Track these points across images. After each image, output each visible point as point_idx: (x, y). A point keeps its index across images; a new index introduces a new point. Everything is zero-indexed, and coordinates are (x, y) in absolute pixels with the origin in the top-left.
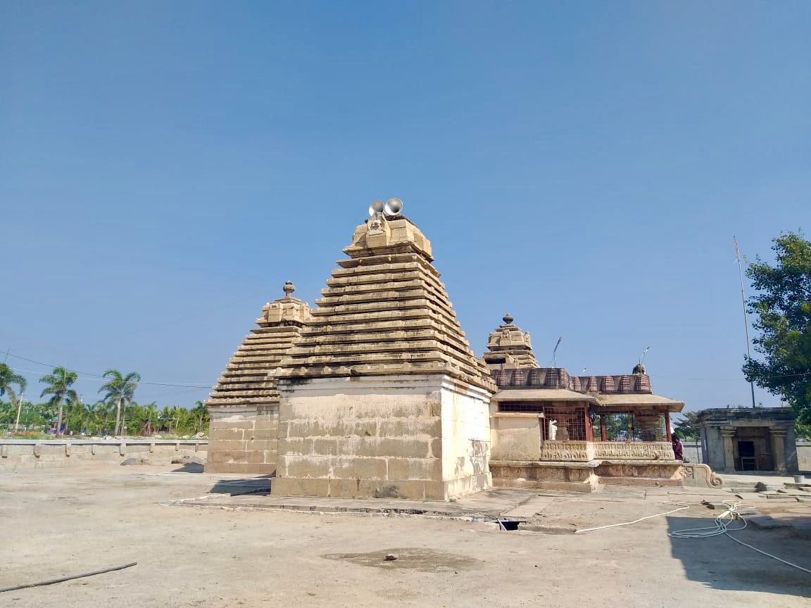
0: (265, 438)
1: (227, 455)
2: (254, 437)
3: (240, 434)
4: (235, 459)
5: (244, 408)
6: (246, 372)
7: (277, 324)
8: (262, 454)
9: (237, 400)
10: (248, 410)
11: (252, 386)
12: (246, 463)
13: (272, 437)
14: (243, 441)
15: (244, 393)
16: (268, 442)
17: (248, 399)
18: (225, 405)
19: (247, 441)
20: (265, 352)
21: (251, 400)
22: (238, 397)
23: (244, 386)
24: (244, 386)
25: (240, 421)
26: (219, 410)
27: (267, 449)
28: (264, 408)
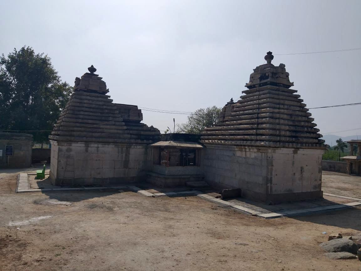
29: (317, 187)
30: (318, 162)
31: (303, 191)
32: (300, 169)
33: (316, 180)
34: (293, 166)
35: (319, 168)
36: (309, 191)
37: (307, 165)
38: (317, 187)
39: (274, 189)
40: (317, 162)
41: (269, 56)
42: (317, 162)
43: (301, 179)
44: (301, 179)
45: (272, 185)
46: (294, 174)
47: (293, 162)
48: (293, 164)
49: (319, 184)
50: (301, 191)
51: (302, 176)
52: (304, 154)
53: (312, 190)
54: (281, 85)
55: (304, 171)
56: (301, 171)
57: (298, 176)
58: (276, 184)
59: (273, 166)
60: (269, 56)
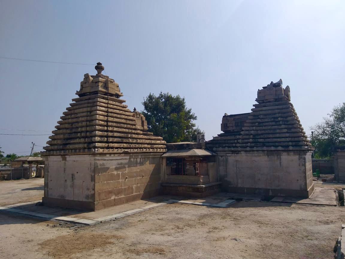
0: (133, 177)
1: (110, 192)
2: (127, 177)
3: (118, 175)
4: (116, 195)
5: (123, 156)
6: (115, 129)
7: (112, 95)
8: (132, 188)
9: (120, 151)
10: (124, 158)
11: (125, 140)
12: (123, 196)
13: (137, 176)
14: (120, 180)
15: (122, 145)
16: (135, 180)
17: (126, 150)
18: (110, 154)
19: (123, 180)
20: (119, 116)
21: (129, 150)
22: (117, 148)
23: (120, 140)
24: (120, 140)
25: (118, 166)
26: (107, 159)
27: (135, 184)
28: (134, 157)
29: (90, 197)
30: (91, 169)
31: (75, 200)
32: (71, 176)
33: (88, 189)
34: (64, 172)
35: (91, 175)
36: (81, 200)
37: (77, 173)
38: (90, 197)
39: (49, 193)
40: (89, 169)
41: (99, 67)
42: (89, 169)
43: (73, 186)
44: (73, 186)
45: (48, 189)
46: (66, 180)
47: (65, 169)
48: (65, 170)
49: (92, 194)
50: (72, 199)
51: (73, 183)
52: (74, 161)
53: (84, 200)
54: (88, 93)
55: (75, 178)
56: (72, 177)
57: (69, 183)
58: (51, 189)
59: (48, 172)
60: (99, 67)
